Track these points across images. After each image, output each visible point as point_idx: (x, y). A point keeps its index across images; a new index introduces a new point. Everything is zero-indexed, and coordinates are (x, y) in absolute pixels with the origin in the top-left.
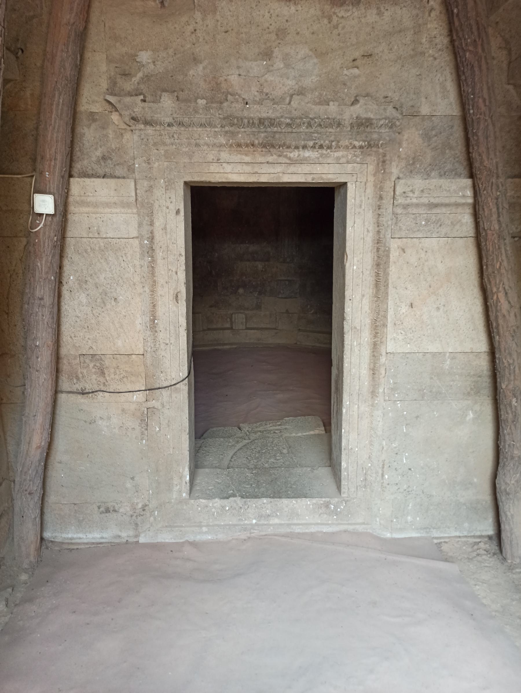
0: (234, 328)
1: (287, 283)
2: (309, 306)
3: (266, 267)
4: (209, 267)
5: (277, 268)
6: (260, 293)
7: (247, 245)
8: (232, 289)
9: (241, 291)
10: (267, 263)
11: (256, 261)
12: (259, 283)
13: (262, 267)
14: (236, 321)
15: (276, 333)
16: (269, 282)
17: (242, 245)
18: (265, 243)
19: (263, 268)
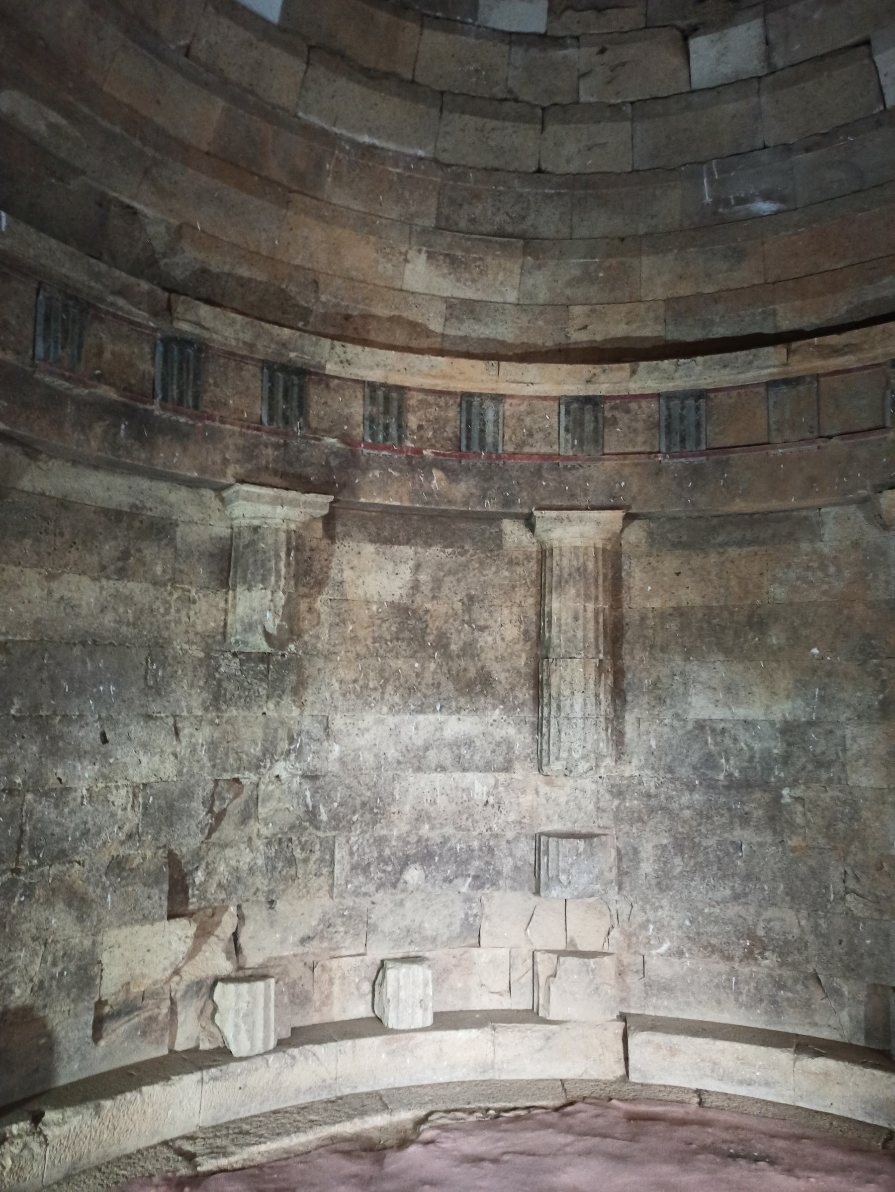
0: (391, 1023)
1: (581, 850)
2: (651, 927)
3: (501, 789)
4: (308, 794)
5: (537, 793)
6: (479, 882)
7: (438, 716)
8: (384, 871)
9: (413, 875)
10: (502, 777)
11: (464, 770)
12: (476, 844)
13: (485, 789)
14: (402, 994)
15: (548, 1038)
16: (508, 842)
17: (421, 717)
18: (497, 711)
19: (488, 794)
